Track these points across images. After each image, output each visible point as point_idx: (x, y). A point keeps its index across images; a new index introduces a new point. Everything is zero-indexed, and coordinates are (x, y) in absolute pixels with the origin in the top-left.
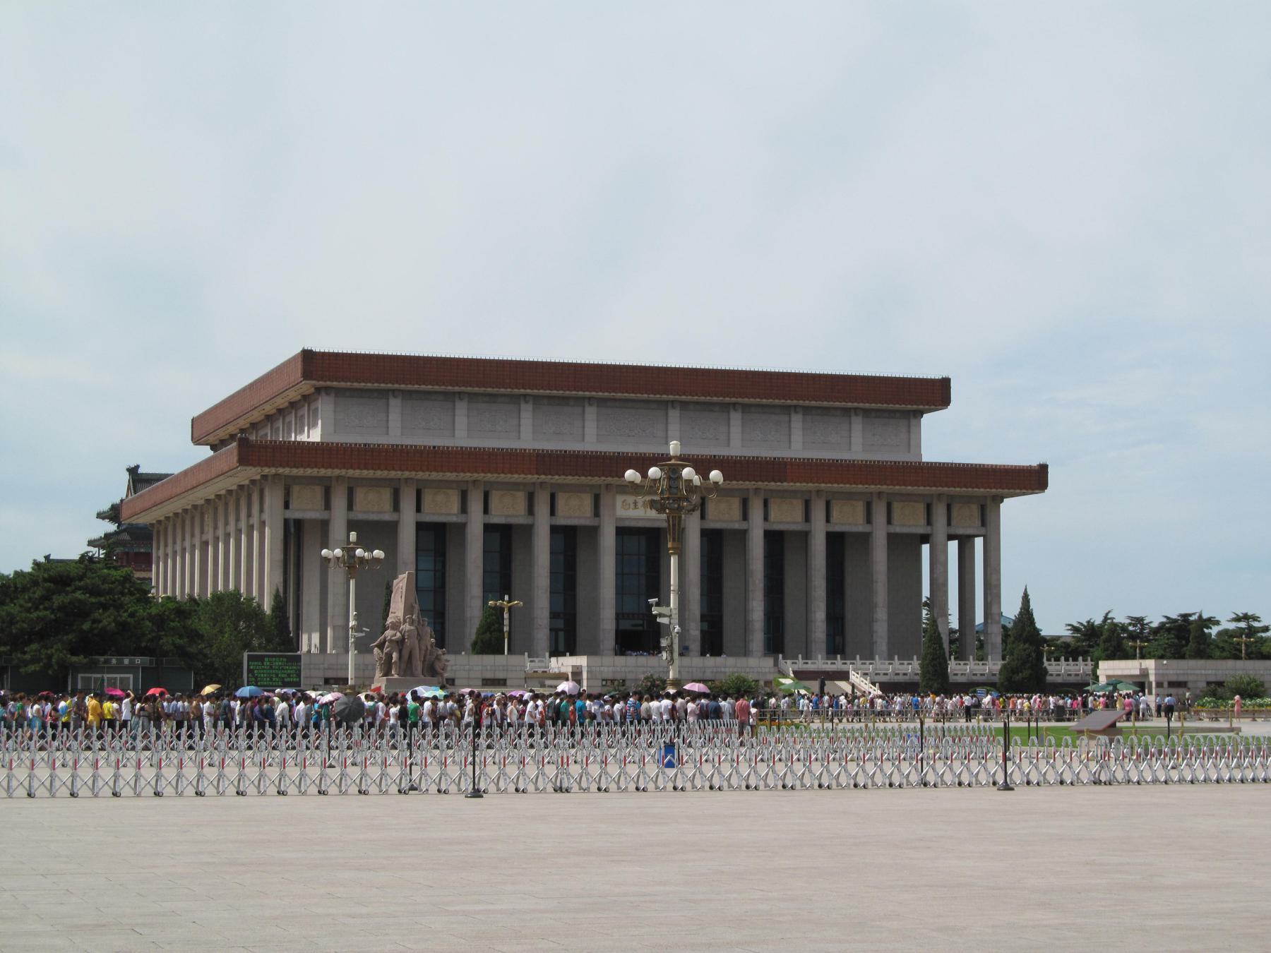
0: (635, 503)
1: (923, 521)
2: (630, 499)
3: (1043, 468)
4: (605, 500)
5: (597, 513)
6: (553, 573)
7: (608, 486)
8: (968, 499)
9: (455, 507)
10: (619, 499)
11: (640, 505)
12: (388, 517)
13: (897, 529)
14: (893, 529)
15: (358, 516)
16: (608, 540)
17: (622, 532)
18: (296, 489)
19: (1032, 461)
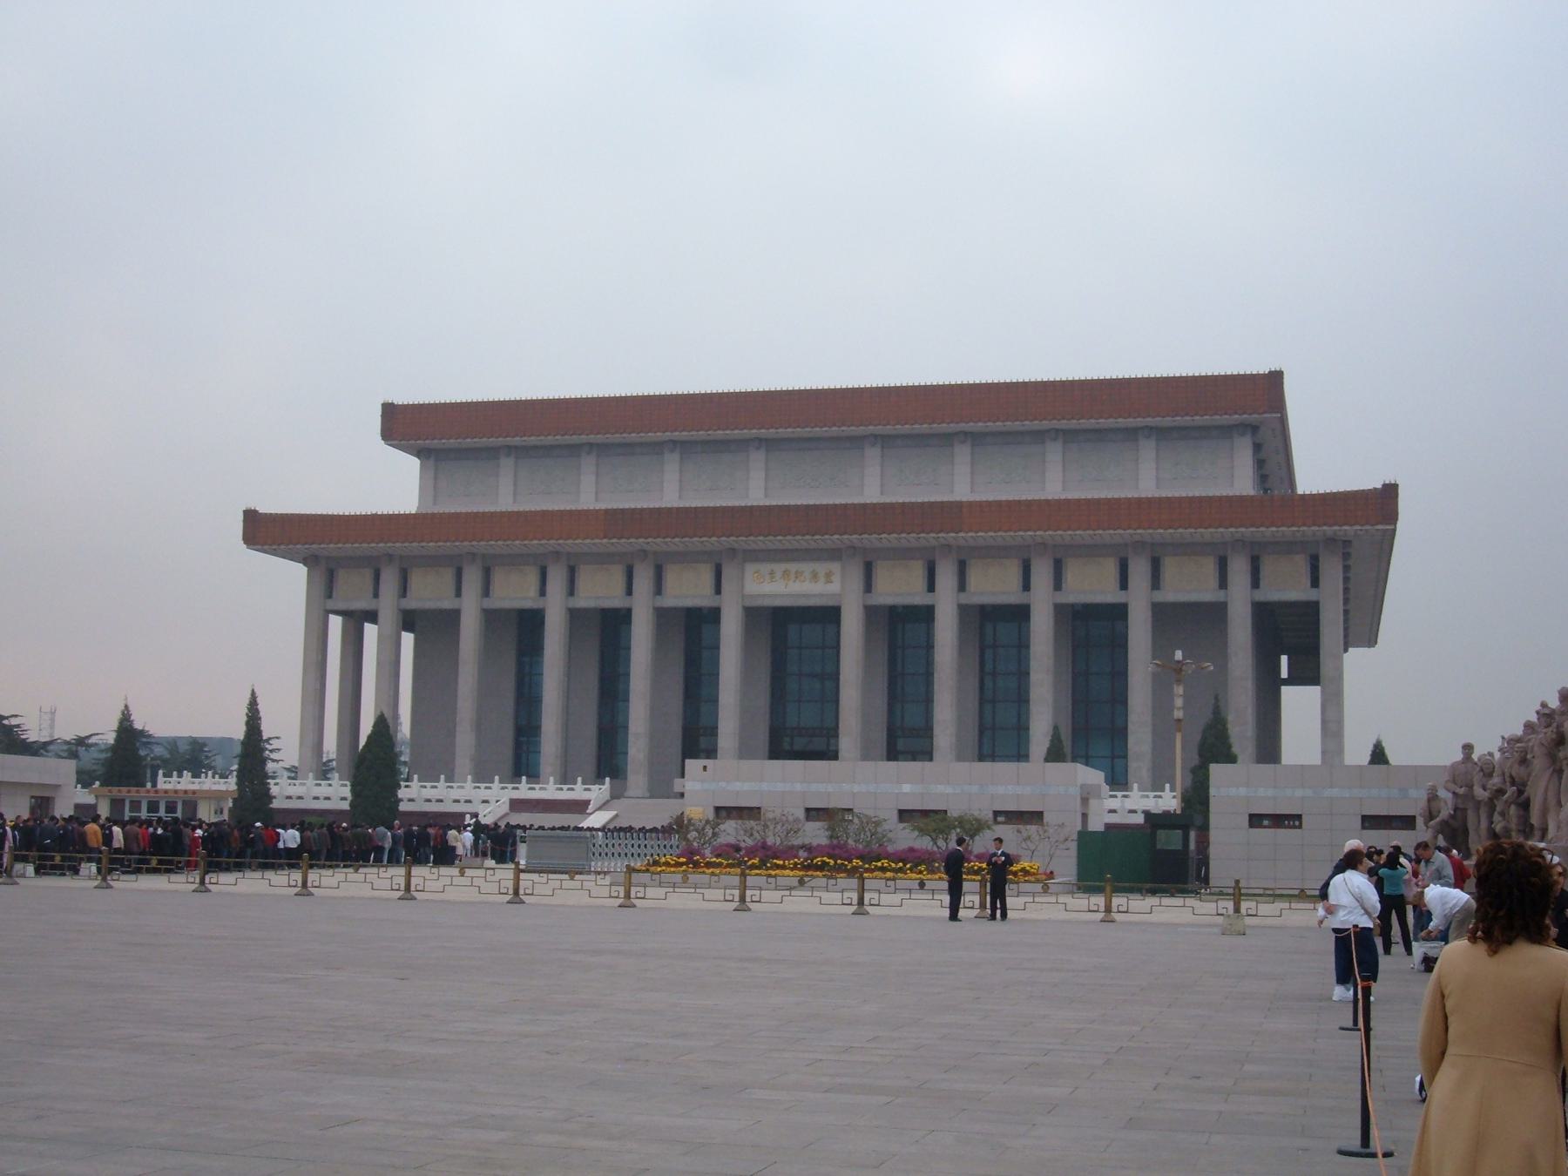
0: (772, 573)
1: (1213, 582)
2: (765, 568)
3: (1390, 491)
4: (727, 572)
5: (718, 591)
6: (715, 676)
7: (733, 552)
8: (1288, 548)
9: (533, 591)
10: (750, 569)
11: (778, 575)
12: (448, 604)
13: (1169, 595)
14: (1160, 597)
15: (411, 603)
16: (731, 629)
17: (754, 615)
18: (342, 576)
19: (1371, 481)
